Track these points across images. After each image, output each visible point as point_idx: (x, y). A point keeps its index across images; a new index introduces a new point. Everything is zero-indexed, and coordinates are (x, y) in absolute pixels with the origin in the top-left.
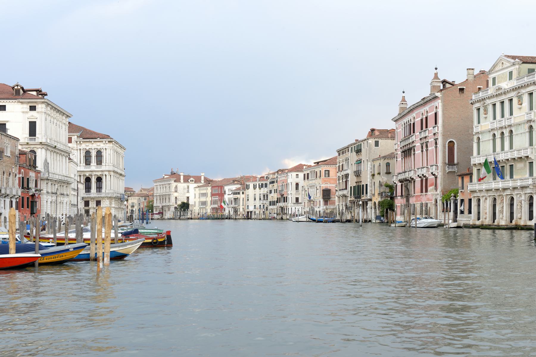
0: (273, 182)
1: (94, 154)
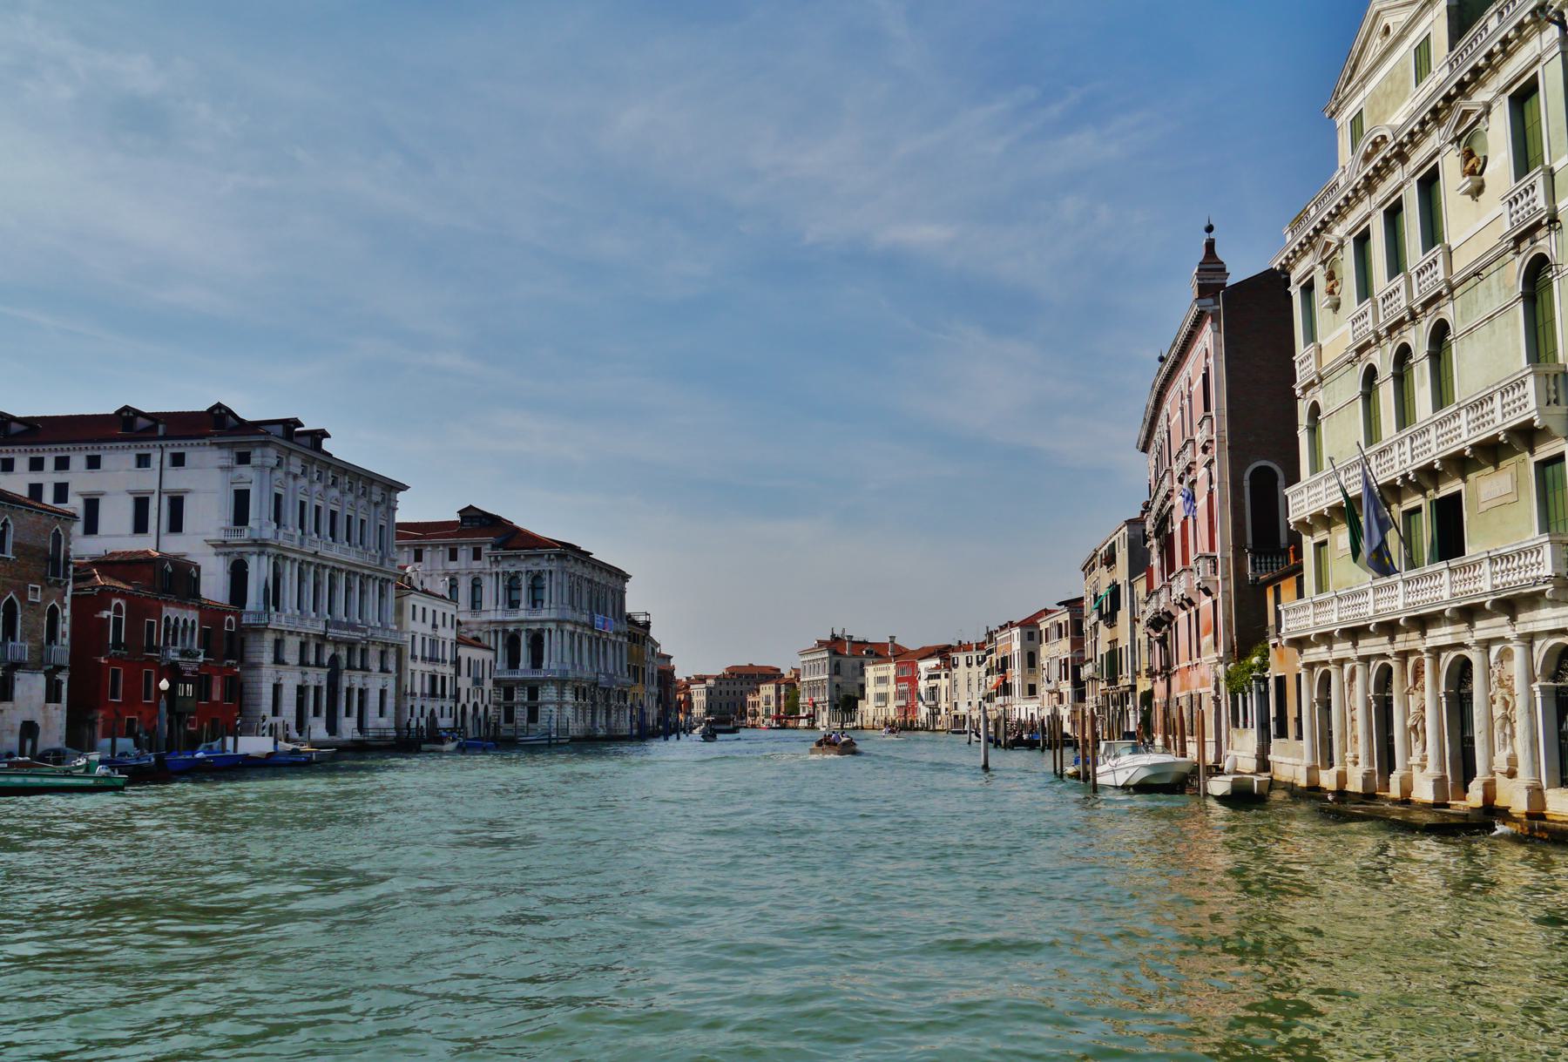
1: (524, 582)
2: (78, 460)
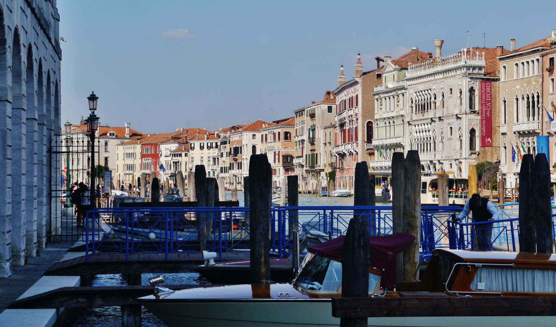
0: (225, 143)
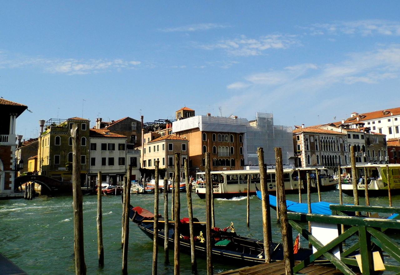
2: (376, 122)
